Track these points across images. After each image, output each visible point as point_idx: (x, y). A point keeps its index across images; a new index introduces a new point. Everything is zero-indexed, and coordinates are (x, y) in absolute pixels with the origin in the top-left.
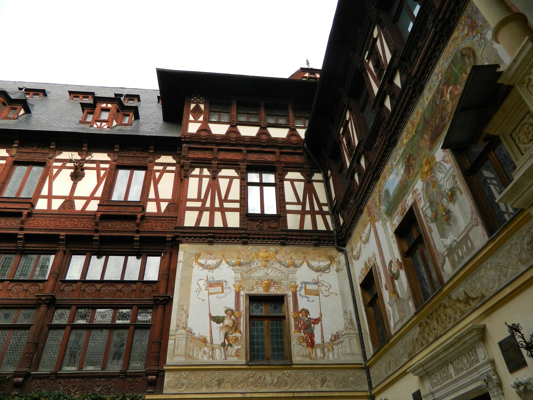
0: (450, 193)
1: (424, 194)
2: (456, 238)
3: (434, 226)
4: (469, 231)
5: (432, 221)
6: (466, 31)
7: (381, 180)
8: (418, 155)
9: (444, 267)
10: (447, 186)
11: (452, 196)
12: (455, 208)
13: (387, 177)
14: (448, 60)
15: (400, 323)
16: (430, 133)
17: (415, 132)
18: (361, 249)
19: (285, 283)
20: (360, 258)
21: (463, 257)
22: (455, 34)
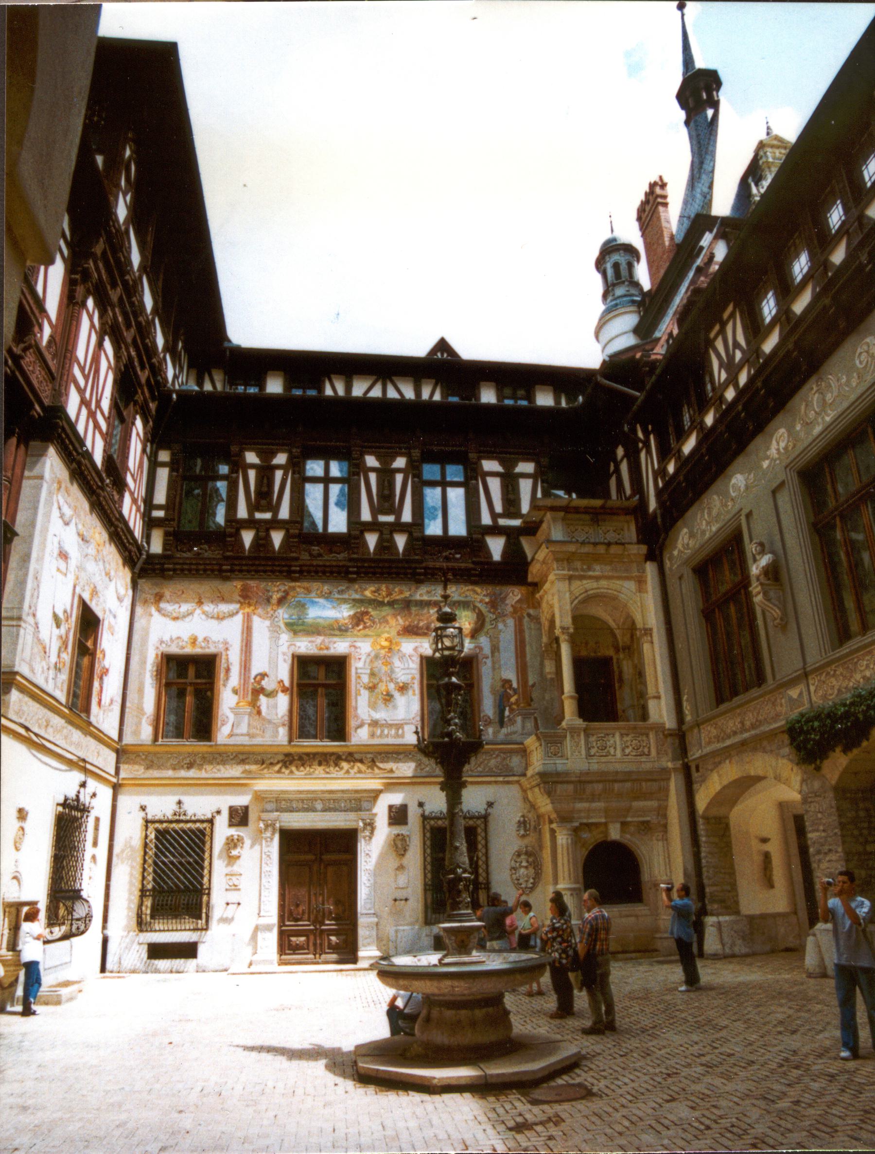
0: (401, 685)
1: (368, 660)
2: (388, 719)
3: (365, 695)
4: (407, 724)
5: (365, 688)
6: (487, 600)
7: (299, 587)
8: (380, 623)
9: (359, 730)
10: (402, 677)
11: (403, 688)
12: (400, 700)
13: (313, 595)
14: (460, 596)
15: (247, 738)
16: (407, 623)
17: (388, 602)
18: (190, 614)
19: (101, 600)
20: (179, 623)
21: (387, 736)
22: (478, 589)
